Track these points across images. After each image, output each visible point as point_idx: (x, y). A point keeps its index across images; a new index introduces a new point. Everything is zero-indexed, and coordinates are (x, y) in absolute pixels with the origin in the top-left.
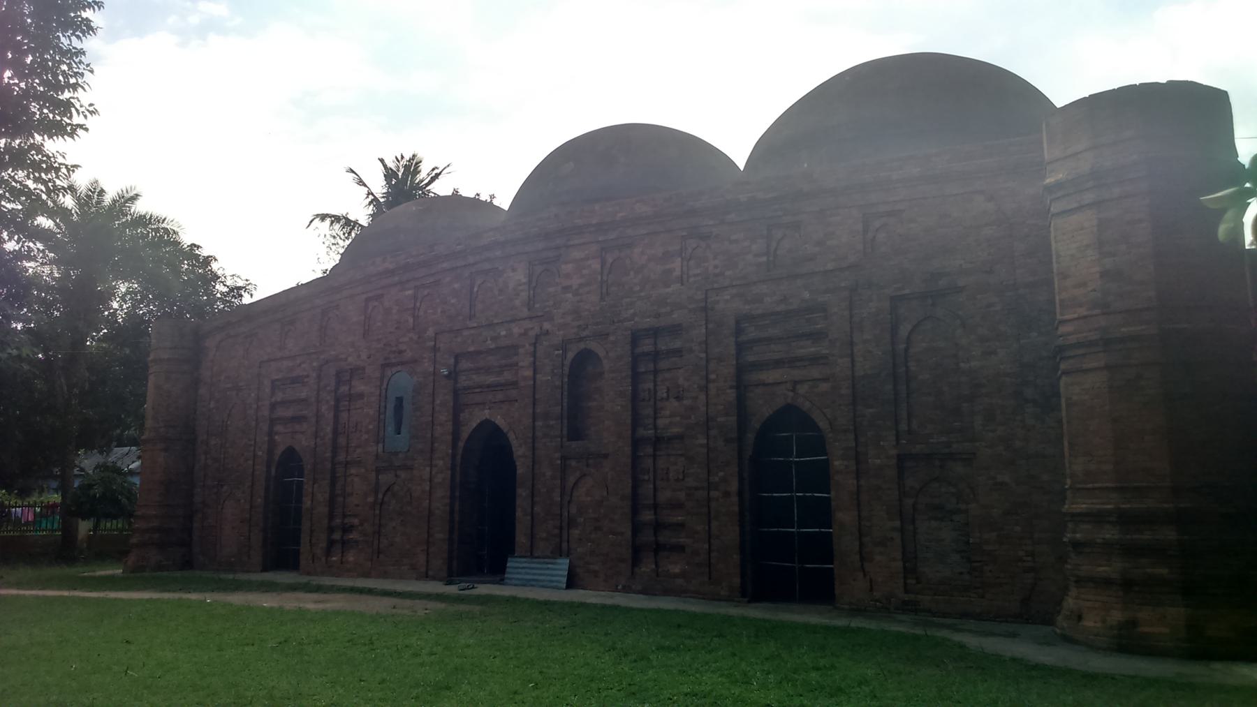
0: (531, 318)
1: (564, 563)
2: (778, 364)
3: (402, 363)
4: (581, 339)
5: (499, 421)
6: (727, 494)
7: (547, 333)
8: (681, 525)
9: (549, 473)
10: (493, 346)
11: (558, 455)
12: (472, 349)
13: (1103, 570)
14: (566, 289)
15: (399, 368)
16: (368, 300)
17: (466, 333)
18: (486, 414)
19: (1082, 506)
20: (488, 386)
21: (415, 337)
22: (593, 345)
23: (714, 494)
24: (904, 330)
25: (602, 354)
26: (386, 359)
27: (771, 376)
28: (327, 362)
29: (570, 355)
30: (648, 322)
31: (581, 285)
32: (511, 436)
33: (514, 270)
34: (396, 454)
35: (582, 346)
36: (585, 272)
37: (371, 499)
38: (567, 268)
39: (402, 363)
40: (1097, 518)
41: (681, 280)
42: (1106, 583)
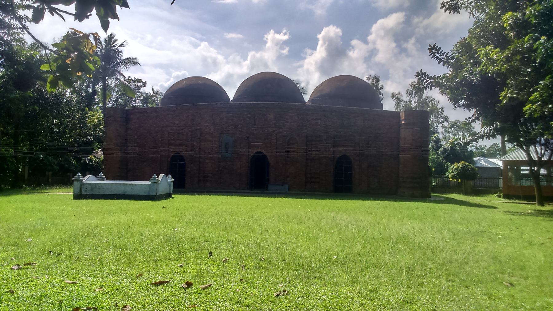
1: (287, 186)
2: (343, 146)
5: (263, 151)
7: (281, 132)
18: (259, 150)
27: (341, 149)
29: (288, 138)
32: (268, 156)
37: (217, 169)
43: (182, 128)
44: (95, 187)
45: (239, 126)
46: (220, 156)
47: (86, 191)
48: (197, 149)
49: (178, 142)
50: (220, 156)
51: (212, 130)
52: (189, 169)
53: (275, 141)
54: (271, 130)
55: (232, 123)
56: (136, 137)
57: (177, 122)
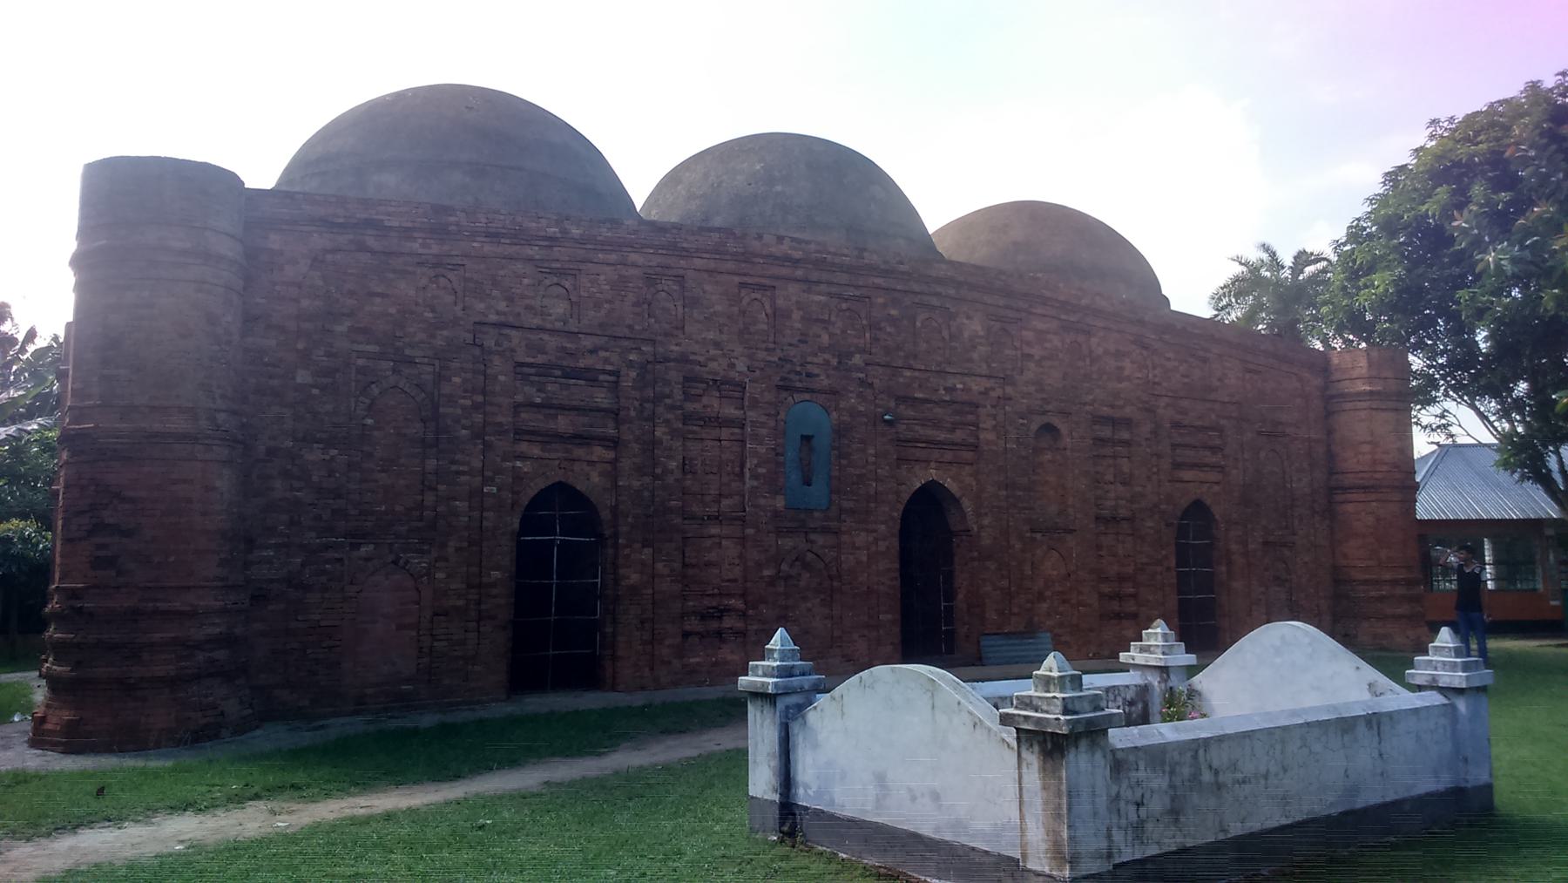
0: (989, 377)
3: (813, 391)
4: (1044, 413)
5: (949, 483)
6: (1168, 569)
8: (1134, 596)
9: (1018, 546)
10: (947, 398)
11: (1026, 528)
12: (920, 395)
13: (1400, 611)
14: (1030, 356)
15: (807, 396)
16: (743, 285)
17: (908, 373)
18: (933, 474)
19: (1388, 576)
20: (940, 442)
21: (834, 362)
22: (1056, 421)
23: (1159, 569)
24: (1262, 454)
25: (1063, 428)
26: (783, 379)
28: (667, 360)
29: (1034, 427)
30: (1106, 411)
31: (1043, 358)
32: (967, 505)
33: (969, 318)
34: (811, 511)
35: (1045, 419)
36: (1048, 345)
37: (766, 573)
38: (1028, 335)
39: (813, 391)
40: (1394, 582)
41: (1128, 379)
42: (1401, 617)
43: (587, 342)
44: (1195, 776)
45: (857, 359)
46: (780, 503)
47: (1138, 829)
48: (673, 464)
49: (563, 424)
50: (780, 503)
51: (741, 366)
52: (634, 578)
53: (991, 436)
54: (975, 388)
55: (825, 339)
56: (303, 377)
57: (560, 308)
